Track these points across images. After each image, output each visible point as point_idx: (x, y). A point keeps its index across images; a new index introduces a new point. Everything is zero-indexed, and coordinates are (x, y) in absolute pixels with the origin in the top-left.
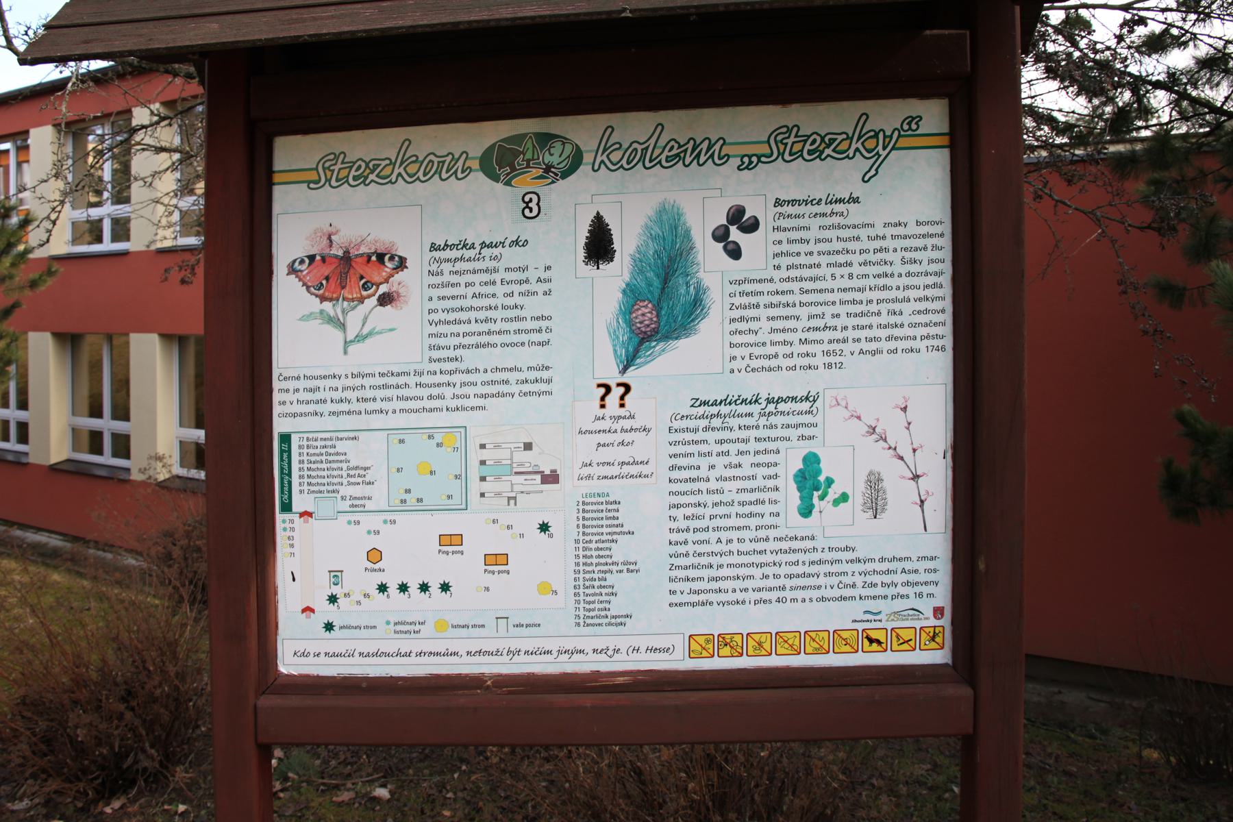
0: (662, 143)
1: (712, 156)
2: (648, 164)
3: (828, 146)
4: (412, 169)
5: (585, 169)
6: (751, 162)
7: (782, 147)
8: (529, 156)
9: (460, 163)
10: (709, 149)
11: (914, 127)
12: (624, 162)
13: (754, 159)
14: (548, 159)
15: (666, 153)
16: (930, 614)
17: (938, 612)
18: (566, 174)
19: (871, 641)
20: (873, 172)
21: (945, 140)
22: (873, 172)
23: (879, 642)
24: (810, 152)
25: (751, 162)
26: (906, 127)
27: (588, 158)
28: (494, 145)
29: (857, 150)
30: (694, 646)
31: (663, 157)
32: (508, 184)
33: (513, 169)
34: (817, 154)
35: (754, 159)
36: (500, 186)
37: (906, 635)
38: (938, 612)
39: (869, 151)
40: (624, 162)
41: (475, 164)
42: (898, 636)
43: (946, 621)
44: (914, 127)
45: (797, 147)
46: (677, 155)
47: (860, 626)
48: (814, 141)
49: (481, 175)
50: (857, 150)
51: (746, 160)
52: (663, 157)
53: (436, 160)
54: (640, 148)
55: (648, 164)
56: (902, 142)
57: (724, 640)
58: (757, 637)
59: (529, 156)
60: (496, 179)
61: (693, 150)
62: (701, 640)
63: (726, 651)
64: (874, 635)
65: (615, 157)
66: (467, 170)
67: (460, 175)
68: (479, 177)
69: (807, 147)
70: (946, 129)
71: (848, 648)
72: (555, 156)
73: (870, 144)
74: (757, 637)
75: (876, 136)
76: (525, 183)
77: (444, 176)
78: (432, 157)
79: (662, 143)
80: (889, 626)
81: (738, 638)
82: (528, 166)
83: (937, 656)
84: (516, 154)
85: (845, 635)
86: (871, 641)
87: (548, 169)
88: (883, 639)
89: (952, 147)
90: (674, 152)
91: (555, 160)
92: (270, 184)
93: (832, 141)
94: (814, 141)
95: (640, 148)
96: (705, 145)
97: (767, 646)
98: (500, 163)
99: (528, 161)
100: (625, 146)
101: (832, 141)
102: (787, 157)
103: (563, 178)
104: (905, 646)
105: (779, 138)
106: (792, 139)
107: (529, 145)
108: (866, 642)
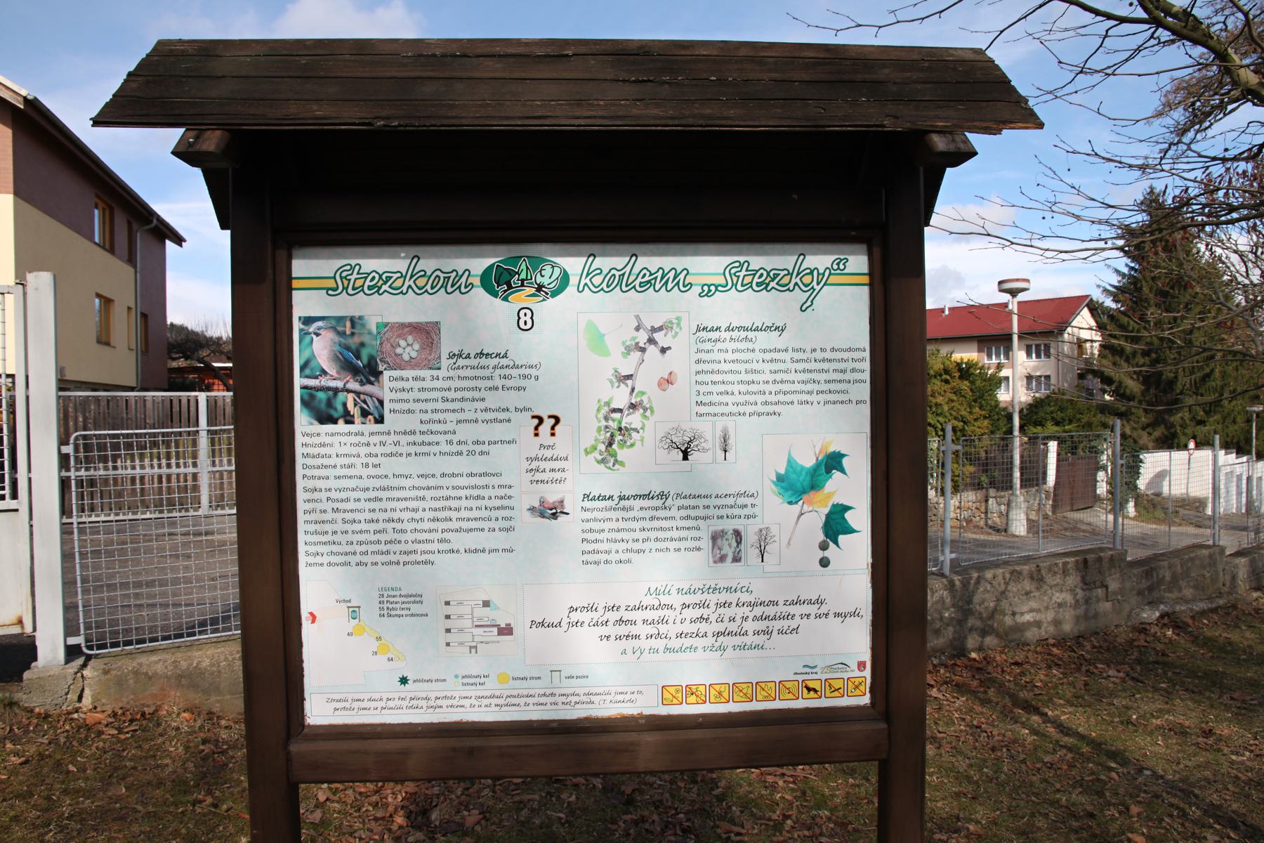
0: (636, 271)
1: (678, 283)
2: (624, 289)
3: (773, 280)
4: (421, 282)
5: (571, 290)
6: (709, 291)
7: (735, 279)
8: (523, 276)
9: (463, 279)
10: (675, 278)
11: (842, 267)
12: (604, 285)
13: (713, 288)
14: (539, 279)
15: (639, 280)
16: (856, 667)
17: (861, 665)
18: (555, 293)
19: (809, 689)
20: (809, 303)
21: (866, 279)
22: (809, 303)
23: (815, 691)
24: (758, 284)
25: (709, 291)
26: (835, 267)
27: (574, 280)
28: (491, 266)
29: (796, 284)
30: (666, 695)
31: (637, 283)
32: (505, 299)
33: (510, 287)
34: (764, 286)
35: (713, 288)
36: (498, 301)
37: (837, 684)
38: (861, 665)
39: (806, 286)
40: (604, 285)
41: (477, 281)
42: (830, 686)
43: (867, 673)
44: (842, 267)
45: (748, 280)
46: (649, 282)
47: (800, 678)
48: (761, 275)
49: (481, 290)
50: (796, 284)
51: (706, 288)
52: (637, 283)
53: (442, 276)
54: (617, 274)
55: (624, 289)
56: (833, 279)
57: (690, 690)
58: (717, 687)
59: (523, 276)
60: (495, 295)
61: (662, 278)
62: (672, 690)
63: (693, 699)
64: (811, 685)
65: (597, 280)
66: (470, 286)
67: (463, 290)
68: (479, 292)
69: (756, 280)
70: (866, 271)
71: (790, 696)
72: (547, 277)
73: (807, 279)
74: (717, 687)
75: (811, 273)
76: (521, 298)
77: (449, 289)
78: (438, 273)
79: (636, 271)
80: (824, 677)
81: (702, 688)
82: (523, 285)
83: (866, 700)
84: (512, 274)
85: (788, 685)
86: (809, 689)
87: (540, 288)
88: (818, 688)
89: (871, 285)
90: (647, 278)
91: (545, 281)
92: (290, 289)
93: (776, 275)
94: (761, 275)
95: (617, 274)
96: (672, 275)
97: (726, 695)
98: (500, 282)
99: (523, 281)
100: (605, 272)
101: (776, 275)
102: (739, 287)
103: (553, 296)
104: (836, 694)
105: (733, 271)
106: (744, 272)
107: (523, 266)
108: (805, 691)
